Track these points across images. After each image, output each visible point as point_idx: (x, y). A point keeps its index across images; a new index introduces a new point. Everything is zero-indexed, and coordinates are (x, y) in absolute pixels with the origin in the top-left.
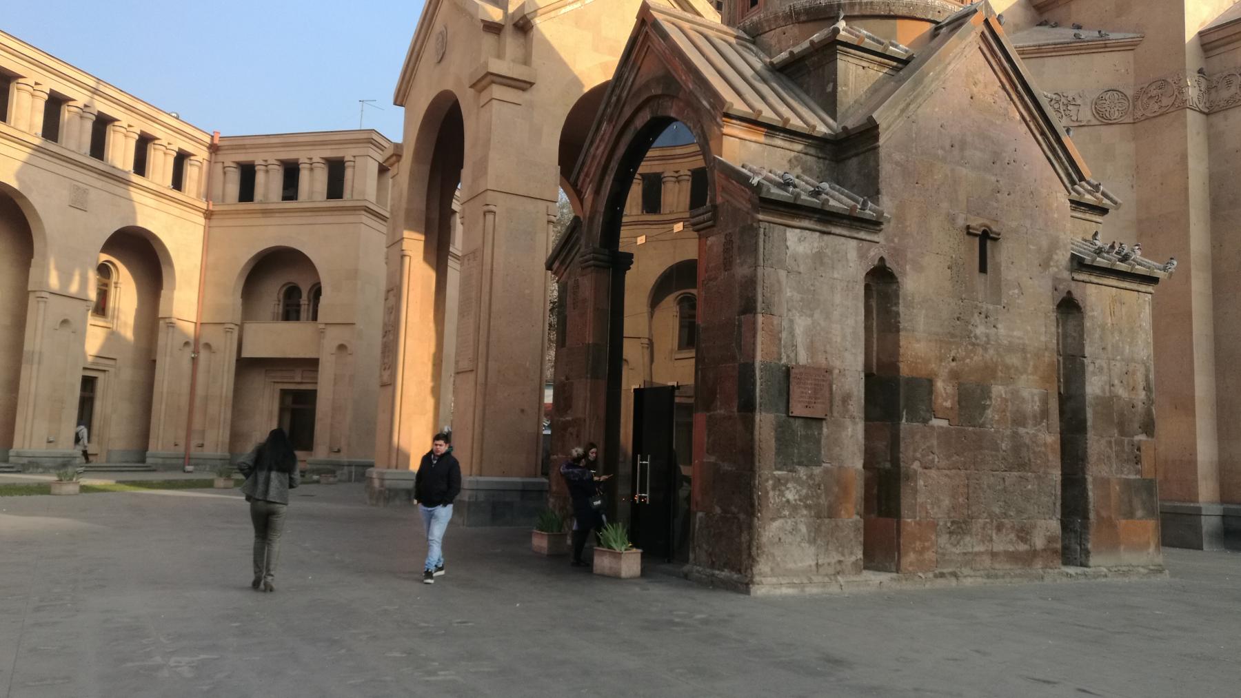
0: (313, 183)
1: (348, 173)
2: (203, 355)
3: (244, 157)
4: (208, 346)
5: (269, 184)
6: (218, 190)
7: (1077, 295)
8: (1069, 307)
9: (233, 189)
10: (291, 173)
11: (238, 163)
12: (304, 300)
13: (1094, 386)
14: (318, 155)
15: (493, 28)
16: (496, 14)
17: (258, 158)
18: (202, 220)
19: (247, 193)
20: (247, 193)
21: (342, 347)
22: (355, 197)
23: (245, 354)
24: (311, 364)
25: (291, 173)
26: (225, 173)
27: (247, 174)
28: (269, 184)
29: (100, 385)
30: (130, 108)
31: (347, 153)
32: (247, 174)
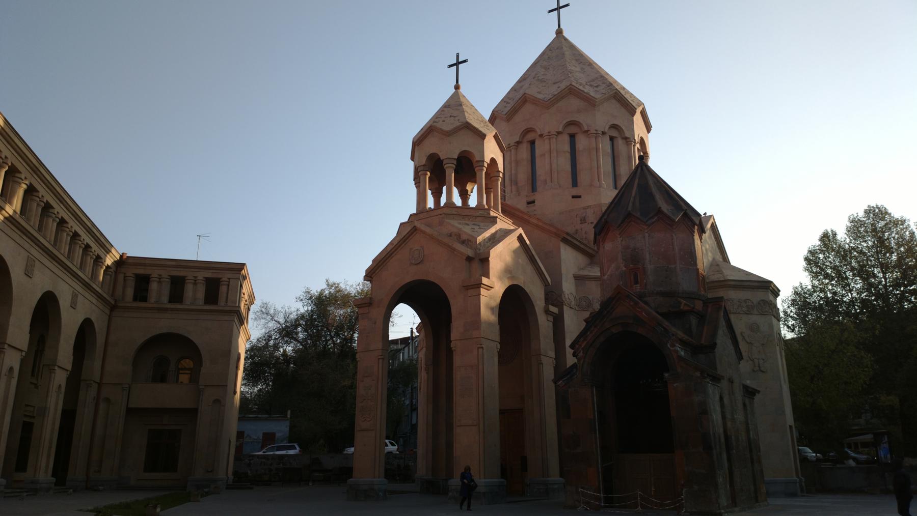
0: (194, 294)
1: (223, 289)
3: (141, 271)
4: (107, 400)
9: (130, 292)
11: (136, 275)
14: (201, 275)
15: (469, 259)
16: (470, 253)
18: (108, 312)
20: (141, 294)
21: (217, 401)
22: (229, 304)
23: (130, 406)
24: (192, 413)
26: (125, 280)
28: (159, 292)
31: (225, 276)
32: (143, 282)
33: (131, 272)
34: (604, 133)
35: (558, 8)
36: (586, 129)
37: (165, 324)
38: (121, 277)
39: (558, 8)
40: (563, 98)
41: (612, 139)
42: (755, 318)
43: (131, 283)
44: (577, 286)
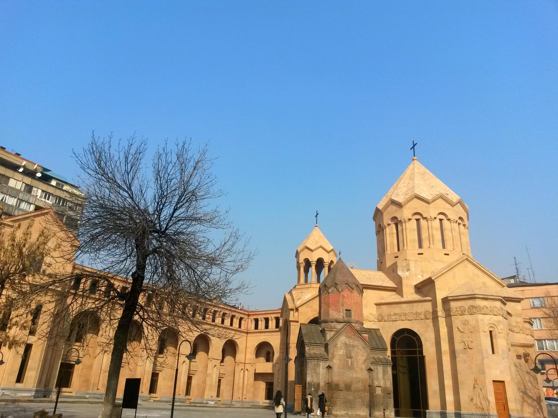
2: (246, 372)
3: (255, 317)
4: (247, 370)
5: (262, 325)
6: (249, 326)
7: (372, 367)
8: (370, 370)
9: (253, 326)
10: (267, 320)
12: (271, 355)
13: (376, 383)
14: (273, 316)
17: (259, 317)
19: (256, 327)
20: (256, 327)
25: (267, 320)
27: (257, 321)
28: (262, 325)
29: (222, 381)
30: (230, 310)
32: (257, 321)
33: (253, 317)
34: (410, 220)
35: (413, 147)
36: (399, 219)
37: (262, 338)
38: (250, 320)
39: (413, 147)
40: (389, 206)
41: (418, 220)
42: (467, 317)
43: (254, 322)
44: (377, 309)
